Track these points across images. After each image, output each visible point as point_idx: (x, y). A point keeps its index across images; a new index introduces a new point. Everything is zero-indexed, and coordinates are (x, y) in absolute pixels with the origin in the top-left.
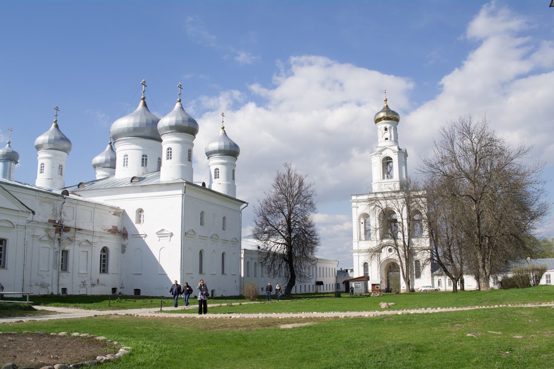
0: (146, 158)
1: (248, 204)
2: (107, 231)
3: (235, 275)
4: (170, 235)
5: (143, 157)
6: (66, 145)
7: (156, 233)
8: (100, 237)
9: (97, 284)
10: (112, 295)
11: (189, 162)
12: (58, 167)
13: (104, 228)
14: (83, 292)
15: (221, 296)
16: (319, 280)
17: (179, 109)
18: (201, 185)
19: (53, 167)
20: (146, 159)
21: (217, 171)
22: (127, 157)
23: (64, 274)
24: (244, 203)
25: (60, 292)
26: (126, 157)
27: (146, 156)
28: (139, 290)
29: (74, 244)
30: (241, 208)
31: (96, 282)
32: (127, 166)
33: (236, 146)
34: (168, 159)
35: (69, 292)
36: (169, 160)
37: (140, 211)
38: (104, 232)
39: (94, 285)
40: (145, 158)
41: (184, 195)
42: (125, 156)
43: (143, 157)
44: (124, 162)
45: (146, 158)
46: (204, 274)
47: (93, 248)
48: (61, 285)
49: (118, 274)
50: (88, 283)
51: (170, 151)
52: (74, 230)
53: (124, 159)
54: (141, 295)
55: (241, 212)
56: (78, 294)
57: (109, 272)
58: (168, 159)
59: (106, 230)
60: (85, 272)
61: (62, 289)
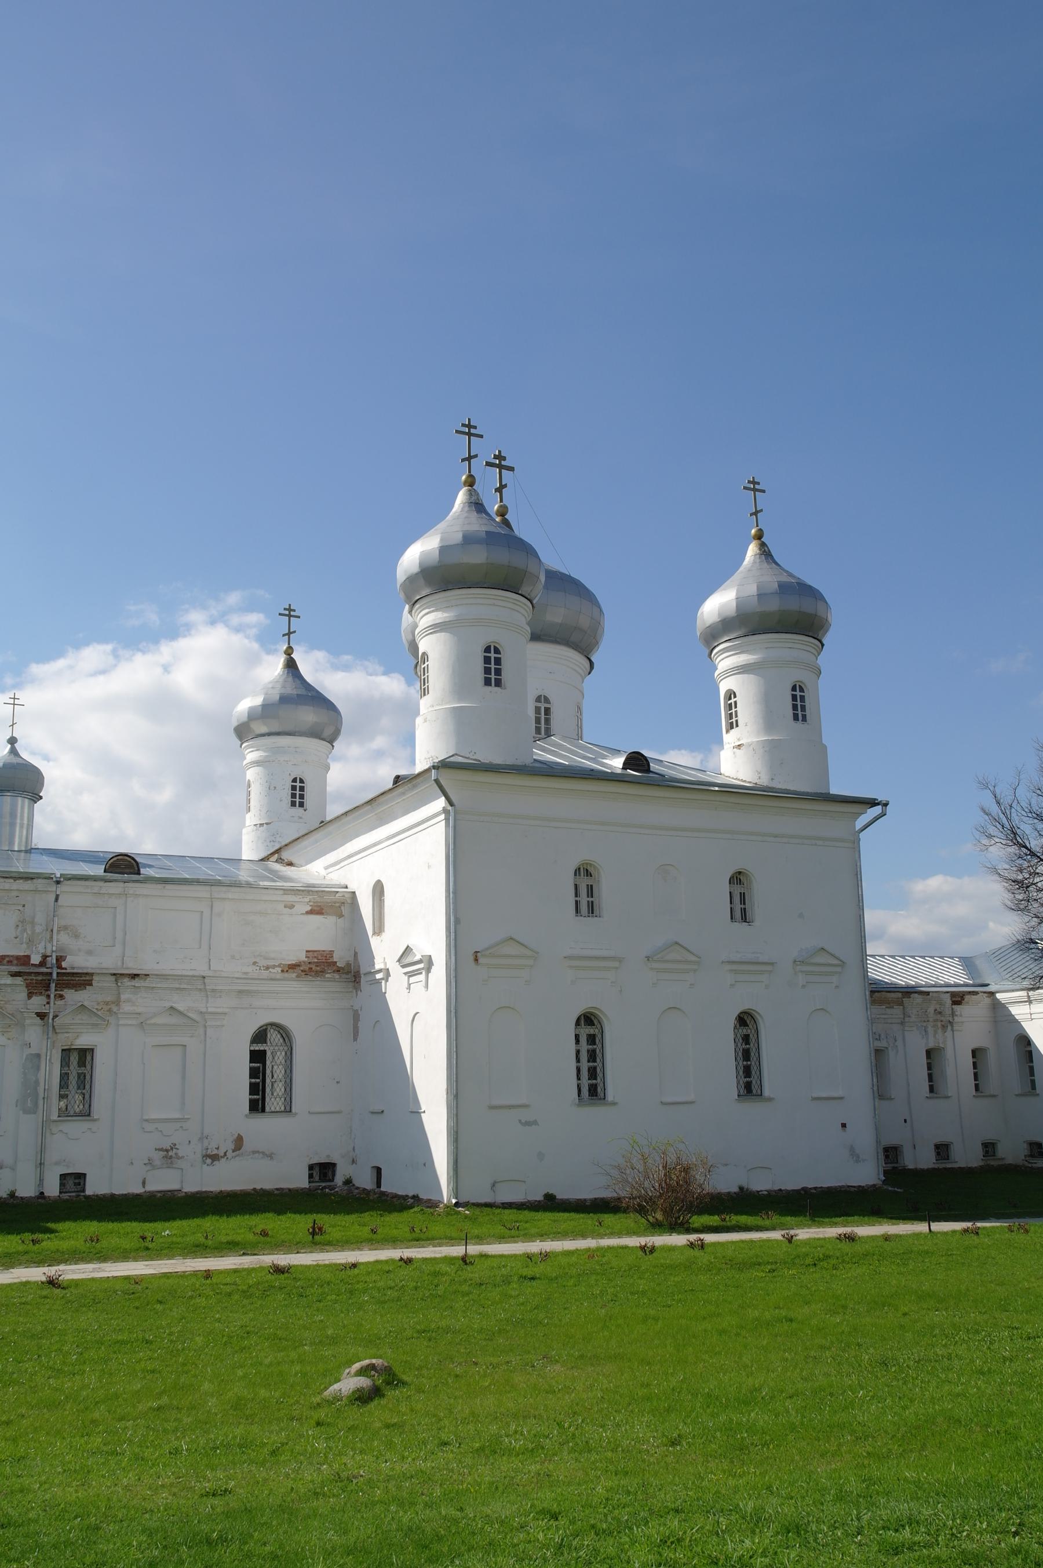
1: (886, 805)
2: (279, 970)
3: (841, 1098)
4: (421, 966)
6: (308, 716)
8: (240, 992)
9: (230, 1154)
10: (309, 1189)
11: (493, 689)
12: (289, 784)
13: (263, 963)
14: (163, 1181)
15: (736, 1190)
17: (467, 509)
18: (617, 763)
19: (271, 788)
21: (732, 701)
23: (76, 1127)
25: (52, 1189)
29: (118, 1025)
31: (229, 1145)
33: (805, 590)
35: (94, 1187)
37: (378, 890)
38: (265, 974)
39: (215, 1158)
41: (452, 813)
46: (614, 1104)
47: (209, 1031)
48: (57, 1163)
49: (339, 1112)
50: (191, 1152)
52: (113, 978)
54: (382, 1189)
56: (138, 1190)
59: (274, 967)
60: (177, 1115)
61: (63, 1177)
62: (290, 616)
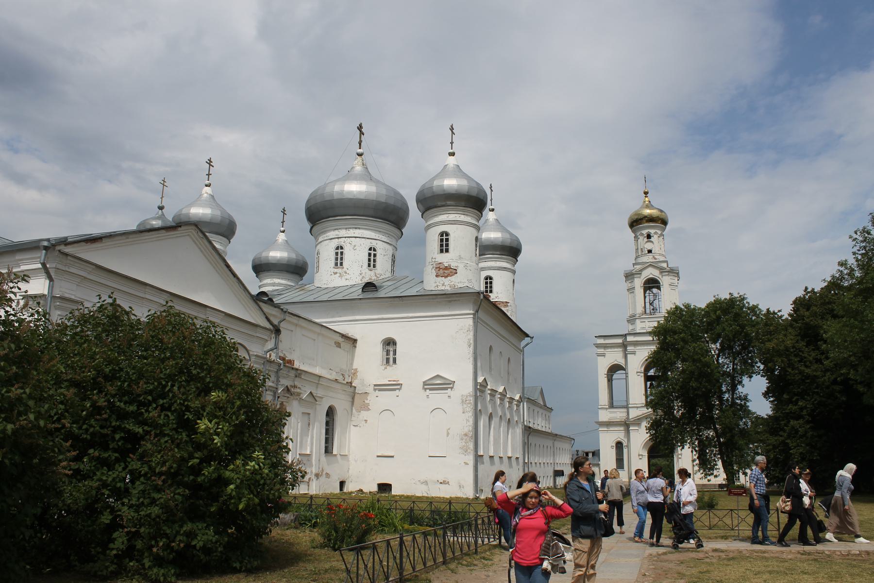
0: (375, 252)
5: (370, 252)
7: (424, 382)
16: (558, 468)
20: (375, 255)
21: (489, 281)
22: (342, 250)
24: (527, 336)
26: (339, 251)
27: (375, 250)
28: (391, 485)
30: (522, 346)
32: (341, 264)
34: (442, 251)
36: (445, 255)
40: (372, 252)
42: (337, 248)
43: (370, 252)
44: (336, 259)
45: (375, 252)
51: (444, 237)
53: (337, 254)
55: (522, 351)
57: (335, 452)
58: (442, 251)
62: (210, 165)
